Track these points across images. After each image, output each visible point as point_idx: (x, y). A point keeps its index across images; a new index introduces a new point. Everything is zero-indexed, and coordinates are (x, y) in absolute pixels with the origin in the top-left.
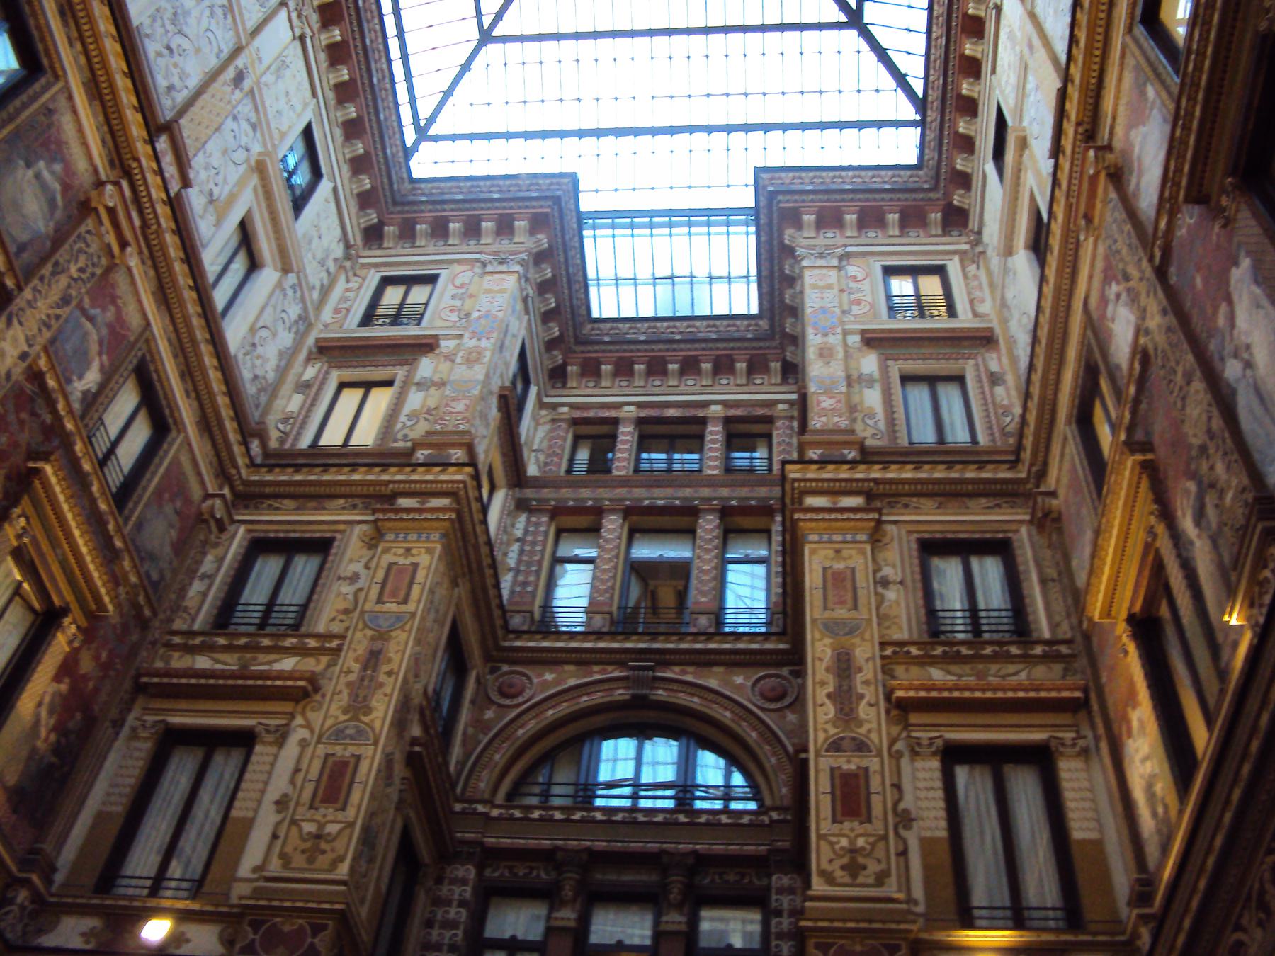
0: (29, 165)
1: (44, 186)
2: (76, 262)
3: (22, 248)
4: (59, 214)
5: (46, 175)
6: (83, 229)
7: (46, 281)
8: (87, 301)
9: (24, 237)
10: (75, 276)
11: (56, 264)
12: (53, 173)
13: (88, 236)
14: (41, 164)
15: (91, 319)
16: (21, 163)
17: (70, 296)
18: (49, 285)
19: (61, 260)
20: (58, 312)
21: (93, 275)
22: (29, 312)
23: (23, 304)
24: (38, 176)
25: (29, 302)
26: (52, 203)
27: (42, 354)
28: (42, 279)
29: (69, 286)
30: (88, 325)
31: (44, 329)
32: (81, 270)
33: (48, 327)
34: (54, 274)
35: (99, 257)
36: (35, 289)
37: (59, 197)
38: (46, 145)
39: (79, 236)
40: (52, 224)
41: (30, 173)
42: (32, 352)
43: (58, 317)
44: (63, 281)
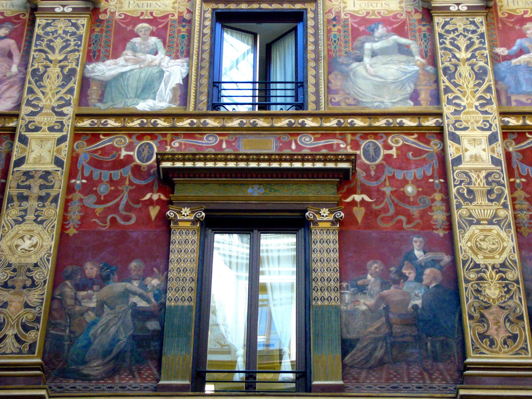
0: (360, 59)
1: (384, 52)
2: (459, 48)
3: (415, 97)
4: (414, 47)
5: (377, 45)
6: (438, 29)
7: (452, 87)
8: (502, 51)
9: (409, 89)
10: (469, 55)
11: (446, 70)
12: (381, 38)
13: (448, 27)
14: (368, 46)
15: (521, 52)
16: (355, 65)
17: (481, 67)
18: (456, 85)
19: (447, 64)
20: (484, 86)
21: (482, 36)
22: (462, 117)
23: (453, 118)
24: (374, 54)
25: (456, 112)
26: (404, 50)
27: (506, 119)
28: (447, 90)
29: (472, 66)
30: (524, 58)
31: (487, 108)
32: (468, 48)
33: (489, 102)
34: (451, 77)
35: (473, 23)
36: (449, 102)
37: (403, 41)
38: (356, 33)
39: (441, 36)
40: (418, 58)
41: (367, 60)
42: (497, 128)
43: (488, 90)
44: (464, 70)
